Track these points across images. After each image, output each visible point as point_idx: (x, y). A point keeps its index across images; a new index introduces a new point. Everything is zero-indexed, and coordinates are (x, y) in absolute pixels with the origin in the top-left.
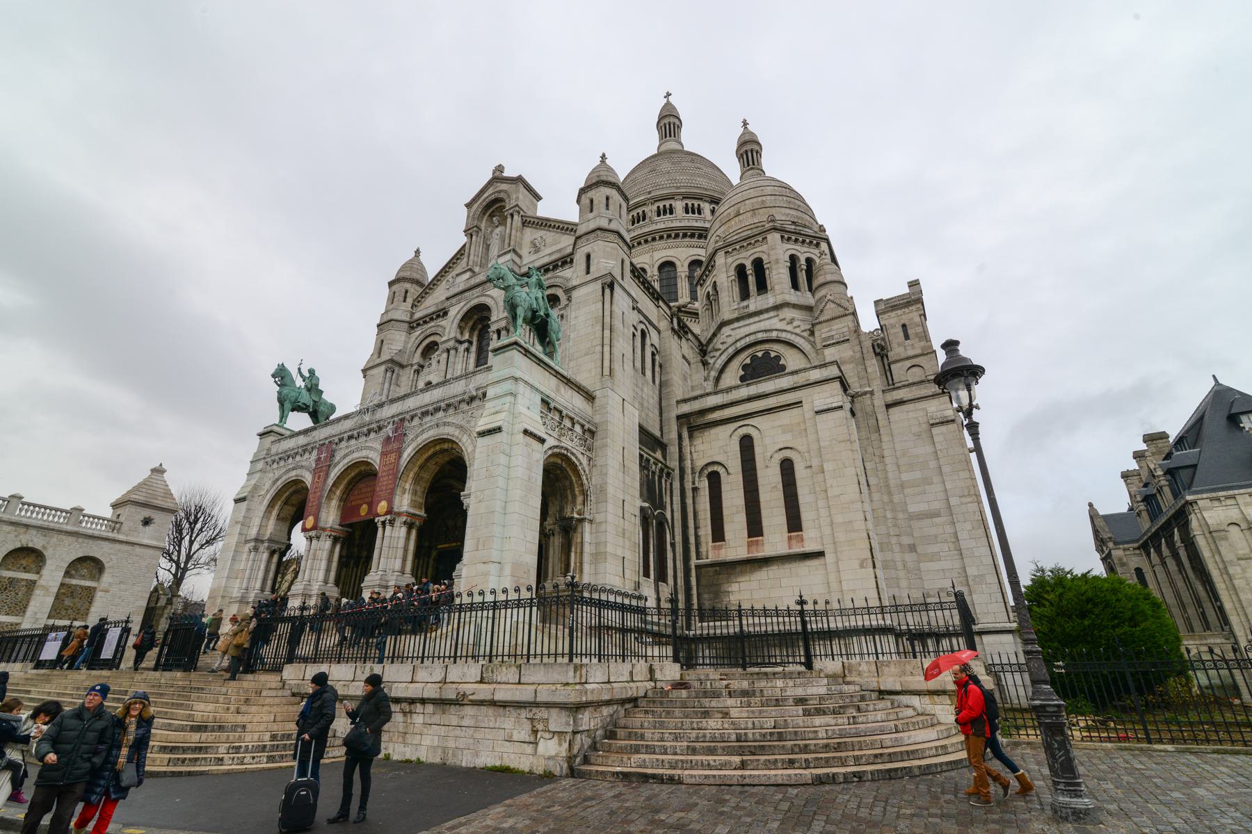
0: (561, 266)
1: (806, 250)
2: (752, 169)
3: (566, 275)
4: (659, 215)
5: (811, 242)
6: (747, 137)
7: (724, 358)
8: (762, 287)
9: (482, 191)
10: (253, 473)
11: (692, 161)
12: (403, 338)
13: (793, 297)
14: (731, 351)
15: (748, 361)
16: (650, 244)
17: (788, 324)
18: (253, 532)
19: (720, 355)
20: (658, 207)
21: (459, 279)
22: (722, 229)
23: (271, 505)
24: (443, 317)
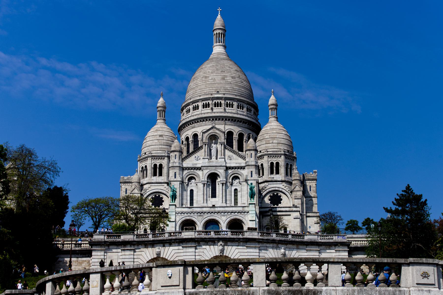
0: (241, 169)
1: (291, 161)
2: (274, 117)
3: (242, 172)
4: (227, 107)
5: (292, 159)
7: (265, 192)
11: (239, 77)
12: (182, 173)
14: (268, 191)
15: (272, 195)
16: (224, 121)
17: (285, 187)
19: (265, 191)
20: (227, 102)
24: (197, 170)
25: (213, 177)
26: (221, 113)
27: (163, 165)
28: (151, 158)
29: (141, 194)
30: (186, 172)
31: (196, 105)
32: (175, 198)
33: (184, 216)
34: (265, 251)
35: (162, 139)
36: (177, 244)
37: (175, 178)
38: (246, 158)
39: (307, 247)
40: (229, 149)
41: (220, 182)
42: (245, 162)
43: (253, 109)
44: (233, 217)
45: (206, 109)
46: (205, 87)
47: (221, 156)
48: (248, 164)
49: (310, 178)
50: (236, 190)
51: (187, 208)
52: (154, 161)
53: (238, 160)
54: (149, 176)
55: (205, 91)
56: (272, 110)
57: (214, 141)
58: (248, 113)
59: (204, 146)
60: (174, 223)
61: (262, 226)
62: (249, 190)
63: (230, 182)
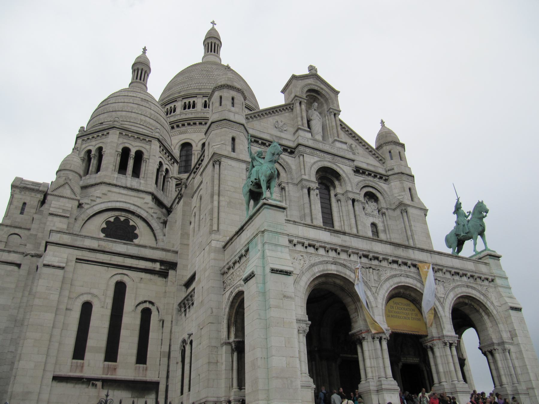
10: (276, 245)
28: (118, 132)
29: (79, 201)
31: (189, 102)
33: (317, 260)
35: (150, 107)
37: (234, 150)
40: (347, 131)
46: (208, 82)
48: (396, 171)
50: (374, 225)
52: (125, 141)
53: (368, 159)
57: (316, 104)
59: (298, 104)
60: (290, 279)
63: (362, 203)
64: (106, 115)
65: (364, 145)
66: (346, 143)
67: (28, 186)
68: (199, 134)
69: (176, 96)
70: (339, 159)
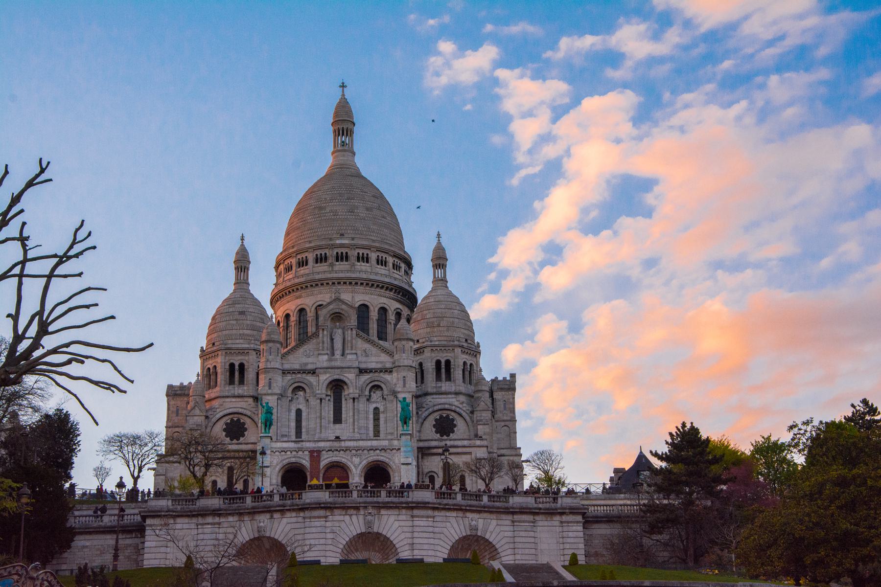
1: (470, 358)
2: (442, 280)
4: (358, 260)
6: (441, 254)
7: (427, 413)
8: (449, 378)
9: (329, 304)
11: (379, 209)
12: (281, 380)
13: (462, 388)
15: (438, 417)
18: (274, 481)
20: (358, 253)
21: (321, 357)
22: (428, 330)
23: (279, 472)
25: (337, 386)
26: (348, 273)
27: (246, 364)
28: (224, 352)
29: (205, 416)
30: (289, 377)
31: (303, 258)
32: (271, 424)
33: (286, 457)
34: (444, 525)
36: (294, 514)
37: (270, 388)
38: (395, 353)
39: (515, 516)
41: (348, 395)
42: (391, 360)
43: (403, 265)
44: (371, 459)
45: (321, 264)
47: (352, 349)
48: (397, 364)
49: (503, 387)
50: (376, 409)
51: (292, 441)
52: (230, 358)
54: (221, 384)
55: (320, 233)
56: (438, 267)
57: (338, 324)
58: (395, 271)
60: (269, 469)
61: (422, 472)
62: (399, 409)
63: (365, 396)
64: (216, 335)
65: (378, 346)
66: (356, 354)
67: (178, 392)
68: (312, 297)
69: (291, 251)
70: (347, 370)
